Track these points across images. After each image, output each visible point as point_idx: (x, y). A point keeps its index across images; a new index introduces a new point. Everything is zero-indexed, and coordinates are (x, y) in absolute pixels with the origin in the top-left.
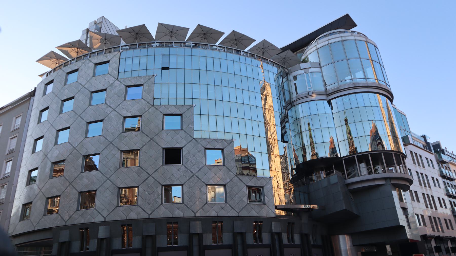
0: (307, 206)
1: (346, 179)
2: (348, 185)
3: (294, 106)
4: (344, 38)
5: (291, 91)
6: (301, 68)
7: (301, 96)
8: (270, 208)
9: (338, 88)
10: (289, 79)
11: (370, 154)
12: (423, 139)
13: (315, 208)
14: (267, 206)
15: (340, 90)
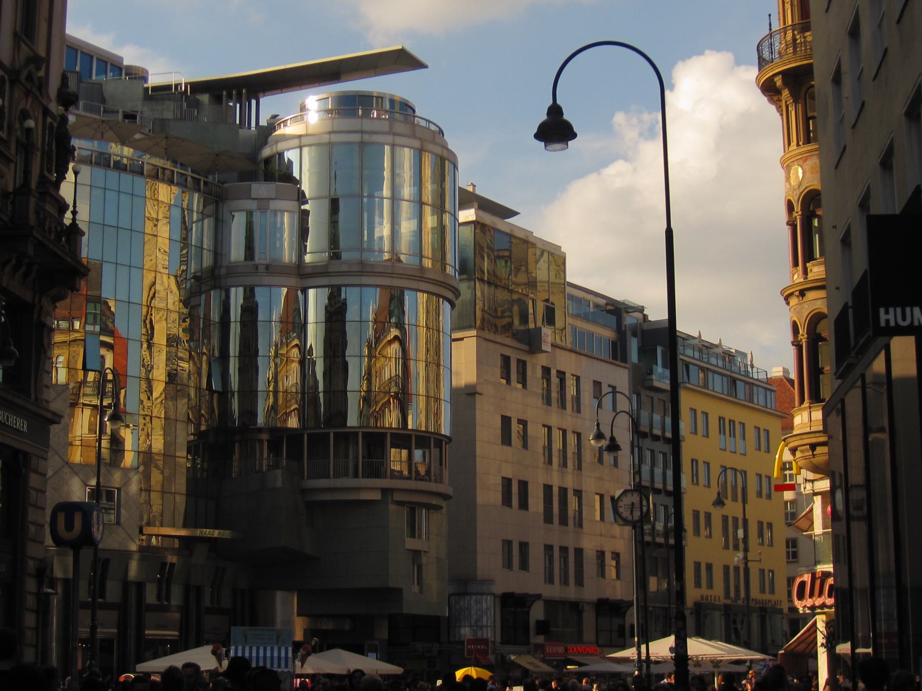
0: (206, 531)
1: (303, 478)
2: (304, 491)
3: (220, 288)
4: (366, 138)
5: (219, 252)
9: (326, 266)
10: (220, 217)
11: (363, 433)
12: (614, 318)
14: (123, 528)
15: (328, 272)
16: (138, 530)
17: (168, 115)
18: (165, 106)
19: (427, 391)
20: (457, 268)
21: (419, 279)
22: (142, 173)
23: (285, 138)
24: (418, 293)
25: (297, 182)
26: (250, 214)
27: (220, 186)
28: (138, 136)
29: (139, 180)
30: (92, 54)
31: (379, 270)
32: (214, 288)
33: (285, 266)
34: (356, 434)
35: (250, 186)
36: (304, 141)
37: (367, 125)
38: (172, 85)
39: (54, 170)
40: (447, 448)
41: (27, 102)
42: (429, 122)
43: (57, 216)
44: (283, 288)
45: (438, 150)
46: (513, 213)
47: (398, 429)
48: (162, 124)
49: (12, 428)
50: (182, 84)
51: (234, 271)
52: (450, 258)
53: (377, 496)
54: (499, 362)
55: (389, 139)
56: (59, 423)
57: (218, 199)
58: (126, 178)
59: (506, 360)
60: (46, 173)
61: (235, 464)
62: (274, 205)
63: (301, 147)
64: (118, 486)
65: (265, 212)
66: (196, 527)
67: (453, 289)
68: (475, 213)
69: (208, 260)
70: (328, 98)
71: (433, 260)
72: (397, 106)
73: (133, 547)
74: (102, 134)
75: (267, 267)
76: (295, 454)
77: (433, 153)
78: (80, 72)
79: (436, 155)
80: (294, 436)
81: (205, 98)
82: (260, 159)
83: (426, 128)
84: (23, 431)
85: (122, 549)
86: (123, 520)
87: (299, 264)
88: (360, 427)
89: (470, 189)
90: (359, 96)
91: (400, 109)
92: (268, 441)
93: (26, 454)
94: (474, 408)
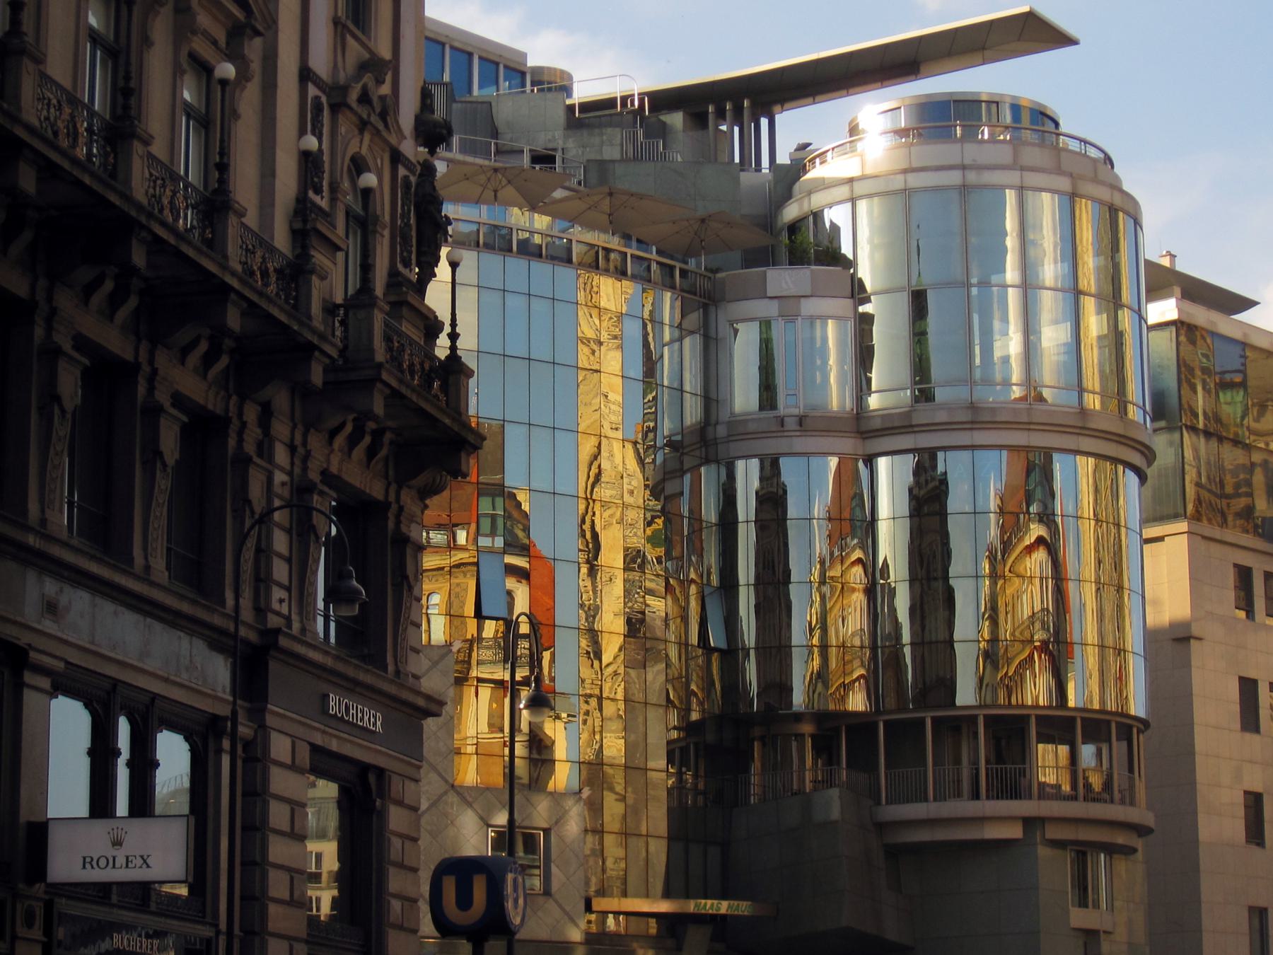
0: (706, 904)
1: (879, 803)
2: (882, 827)
3: (718, 462)
4: (972, 177)
5: (713, 395)
6: (769, 295)
7: (752, 427)
8: (568, 908)
9: (908, 415)
10: (713, 334)
11: (985, 716)
13: (736, 913)
14: (556, 902)
15: (912, 426)
16: (582, 905)
17: (612, 153)
18: (605, 137)
19: (1101, 635)
20: (1148, 408)
21: (1078, 431)
22: (569, 261)
23: (824, 185)
24: (1078, 457)
25: (848, 264)
26: (766, 324)
27: (710, 278)
28: (559, 194)
29: (564, 273)
30: (470, 49)
31: (1003, 419)
32: (707, 461)
33: (831, 418)
34: (973, 720)
35: (765, 273)
36: (859, 188)
37: (971, 153)
38: (615, 99)
39: (414, 261)
40: (1141, 741)
41: (361, 142)
42: (1086, 142)
43: (422, 343)
44: (829, 458)
45: (1104, 194)
46: (1247, 304)
47: (1050, 707)
48: (600, 170)
49: (356, 725)
50: (633, 95)
51: (740, 430)
52: (1133, 390)
53: (1015, 832)
54: (1230, 577)
55: (1013, 177)
56: (437, 715)
57: (704, 301)
58: (541, 269)
59: (1244, 575)
60: (400, 267)
61: (754, 780)
62: (810, 307)
63: (853, 201)
64: (545, 825)
65: (793, 321)
66: (688, 895)
67: (1143, 449)
68: (1177, 306)
69: (693, 412)
70: (900, 108)
71: (1104, 395)
72: (1026, 119)
73: (576, 935)
74: (496, 191)
75: (801, 420)
76: (863, 759)
77: (1094, 200)
78: (451, 83)
79: (1101, 202)
80: (860, 726)
81: (676, 119)
82: (780, 224)
83: (1079, 154)
84: (374, 732)
85: (555, 938)
86: (555, 886)
87: (857, 414)
88: (980, 707)
89: (1166, 262)
90: (955, 101)
91: (1032, 123)
92: (813, 737)
93: (380, 772)
94: (1187, 665)
